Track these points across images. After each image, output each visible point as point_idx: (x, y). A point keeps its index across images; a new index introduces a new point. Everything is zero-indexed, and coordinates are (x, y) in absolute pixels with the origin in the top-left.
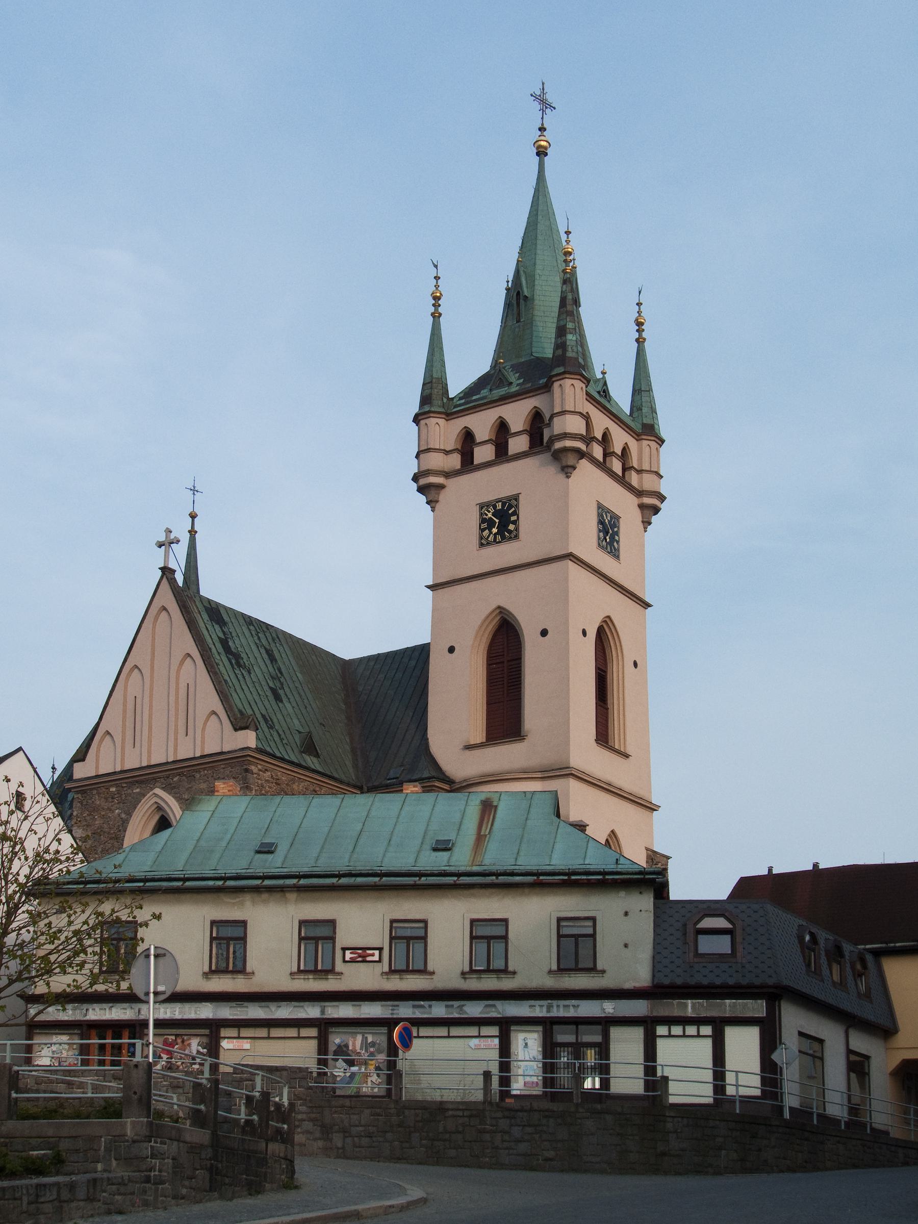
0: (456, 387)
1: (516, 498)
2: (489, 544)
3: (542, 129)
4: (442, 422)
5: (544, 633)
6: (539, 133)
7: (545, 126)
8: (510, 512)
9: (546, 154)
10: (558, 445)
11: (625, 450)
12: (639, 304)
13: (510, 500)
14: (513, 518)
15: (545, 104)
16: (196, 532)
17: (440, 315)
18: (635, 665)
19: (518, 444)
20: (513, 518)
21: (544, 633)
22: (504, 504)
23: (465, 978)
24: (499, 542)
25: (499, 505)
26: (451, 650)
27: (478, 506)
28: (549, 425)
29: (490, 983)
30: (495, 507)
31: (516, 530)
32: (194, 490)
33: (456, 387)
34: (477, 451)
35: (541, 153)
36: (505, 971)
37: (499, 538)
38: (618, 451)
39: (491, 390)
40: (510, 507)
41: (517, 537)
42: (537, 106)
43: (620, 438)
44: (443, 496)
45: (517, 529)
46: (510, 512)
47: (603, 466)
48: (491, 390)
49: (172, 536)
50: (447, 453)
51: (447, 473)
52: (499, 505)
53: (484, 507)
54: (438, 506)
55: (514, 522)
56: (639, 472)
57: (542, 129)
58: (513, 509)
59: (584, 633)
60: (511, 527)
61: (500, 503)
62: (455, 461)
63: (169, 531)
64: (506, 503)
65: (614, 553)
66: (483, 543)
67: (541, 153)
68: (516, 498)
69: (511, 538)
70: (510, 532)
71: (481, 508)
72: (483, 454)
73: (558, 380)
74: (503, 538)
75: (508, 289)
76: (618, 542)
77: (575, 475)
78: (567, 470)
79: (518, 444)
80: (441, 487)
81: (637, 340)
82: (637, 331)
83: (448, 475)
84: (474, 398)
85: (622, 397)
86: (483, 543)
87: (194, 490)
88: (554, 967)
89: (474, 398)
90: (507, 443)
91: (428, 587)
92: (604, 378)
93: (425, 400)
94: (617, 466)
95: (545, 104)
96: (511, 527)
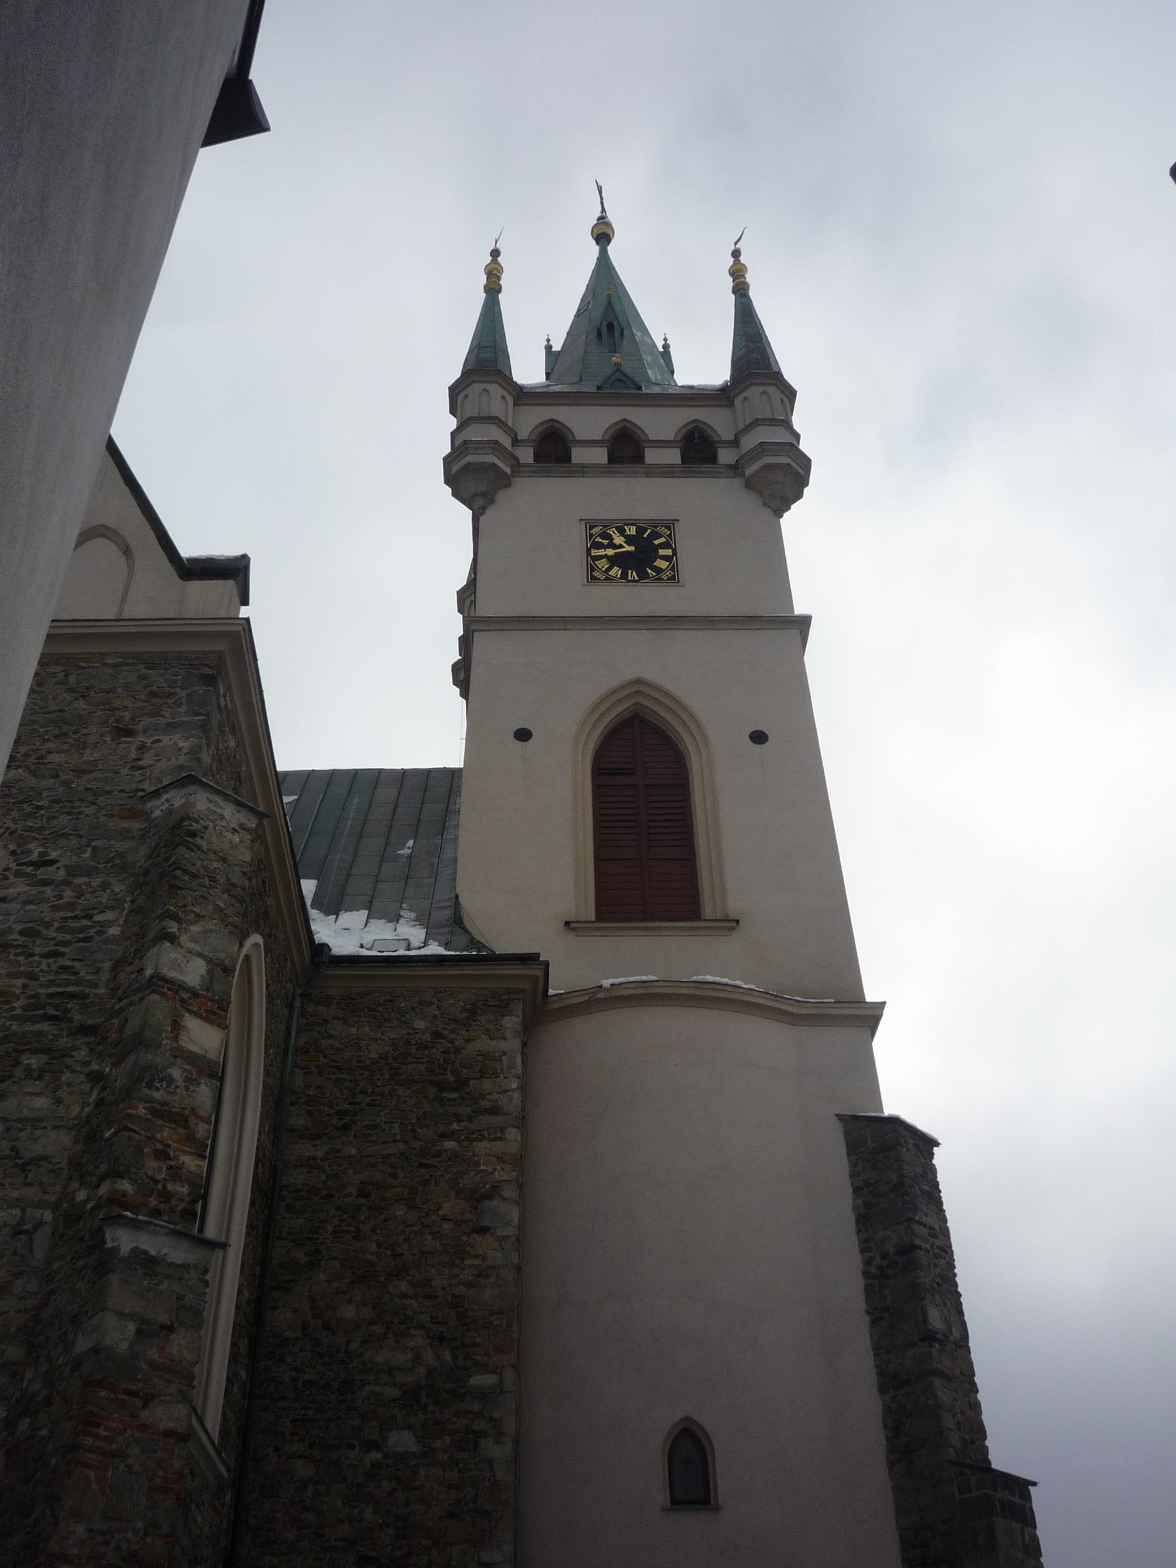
8: (656, 542)
13: (656, 527)
20: (662, 552)
22: (641, 530)
24: (637, 581)
25: (632, 531)
27: (583, 524)
28: (735, 443)
31: (672, 569)
44: (502, 497)
46: (656, 542)
52: (632, 531)
53: (597, 526)
55: (665, 558)
58: (663, 540)
60: (662, 564)
61: (633, 529)
62: (526, 455)
69: (660, 579)
70: (658, 570)
73: (762, 384)
75: (548, 348)
83: (518, 467)
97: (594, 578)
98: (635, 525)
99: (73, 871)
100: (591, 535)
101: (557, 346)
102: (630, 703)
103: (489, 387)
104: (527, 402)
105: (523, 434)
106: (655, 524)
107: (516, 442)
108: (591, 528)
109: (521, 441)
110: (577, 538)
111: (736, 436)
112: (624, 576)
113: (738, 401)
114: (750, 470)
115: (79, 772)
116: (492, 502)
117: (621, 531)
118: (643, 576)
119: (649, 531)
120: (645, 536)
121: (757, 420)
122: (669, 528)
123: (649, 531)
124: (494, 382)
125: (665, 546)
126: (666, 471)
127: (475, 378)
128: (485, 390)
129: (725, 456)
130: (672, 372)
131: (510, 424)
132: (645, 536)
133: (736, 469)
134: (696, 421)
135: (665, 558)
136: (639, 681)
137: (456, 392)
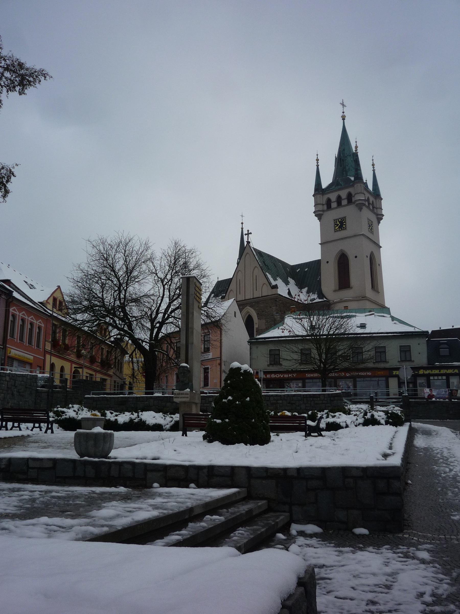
0: (324, 185)
1: (345, 218)
2: (337, 231)
4: (321, 196)
5: (356, 257)
6: (342, 114)
7: (344, 111)
9: (345, 119)
10: (357, 202)
11: (373, 202)
12: (373, 160)
14: (344, 223)
15: (343, 105)
16: (243, 228)
17: (319, 165)
18: (379, 265)
19: (344, 202)
20: (344, 223)
21: (356, 257)
22: (341, 220)
23: (374, 364)
25: (340, 220)
26: (328, 262)
28: (354, 196)
29: (382, 365)
30: (338, 220)
32: (242, 216)
33: (324, 185)
34: (332, 204)
35: (344, 119)
36: (386, 362)
37: (340, 229)
38: (371, 203)
39: (335, 187)
40: (343, 220)
41: (346, 229)
42: (342, 106)
43: (371, 199)
45: (346, 227)
47: (368, 207)
48: (335, 187)
49: (249, 232)
50: (323, 205)
51: (324, 210)
52: (340, 220)
55: (345, 225)
56: (377, 208)
57: (343, 112)
59: (367, 256)
60: (344, 226)
62: (325, 207)
63: (248, 231)
65: (372, 233)
66: (335, 231)
67: (344, 119)
68: (345, 218)
71: (334, 221)
72: (334, 205)
74: (342, 229)
75: (336, 157)
76: (373, 229)
77: (363, 210)
78: (360, 209)
79: (344, 202)
80: (322, 214)
81: (373, 170)
82: (373, 168)
83: (323, 211)
84: (331, 189)
85: (370, 187)
86: (335, 231)
87: (242, 216)
88: (400, 360)
89: (331, 189)
90: (341, 201)
91: (320, 244)
92: (366, 182)
93: (316, 190)
94: (371, 207)
95: (343, 105)
96: (344, 226)
97: (335, 231)
99: (270, 321)
102: (341, 253)
106: (343, 218)
107: (323, 205)
108: (334, 221)
110: (332, 223)
112: (339, 229)
114: (356, 203)
115: (268, 312)
116: (321, 219)
118: (342, 229)
122: (345, 218)
125: (345, 222)
126: (345, 206)
129: (353, 200)
133: (354, 203)
135: (345, 225)
136: (341, 250)
137: (314, 196)
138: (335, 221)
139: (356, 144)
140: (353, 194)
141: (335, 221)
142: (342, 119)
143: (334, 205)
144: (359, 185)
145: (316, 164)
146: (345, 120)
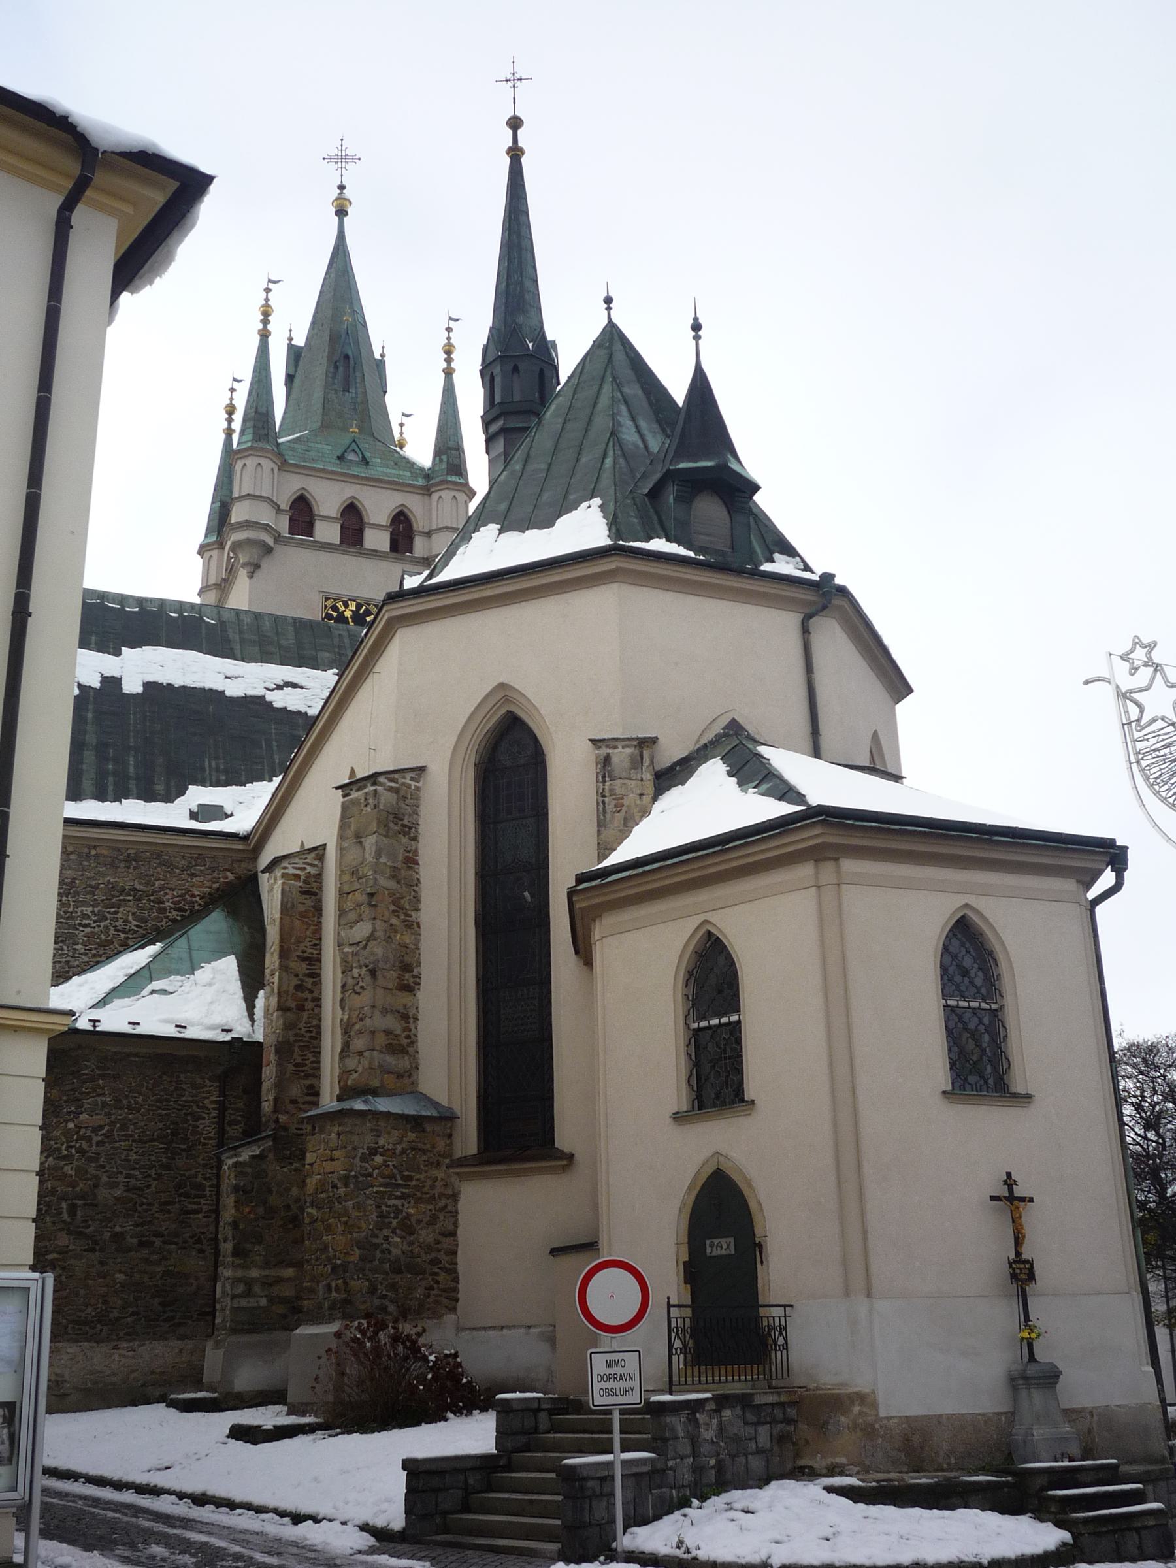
3: (342, 187)
4: (276, 470)
6: (339, 191)
9: (346, 214)
13: (369, 605)
22: (359, 606)
28: (428, 534)
35: (341, 212)
53: (330, 599)
54: (258, 574)
57: (342, 187)
64: (362, 606)
67: (341, 212)
75: (291, 339)
79: (377, 539)
80: (269, 550)
83: (278, 538)
98: (354, 601)
100: (326, 606)
101: (300, 341)
103: (263, 461)
104: (287, 469)
105: (283, 507)
107: (279, 510)
108: (327, 599)
109: (283, 510)
111: (430, 531)
113: (435, 496)
117: (346, 605)
119: (364, 607)
120: (361, 612)
121: (446, 527)
123: (364, 607)
124: (266, 457)
127: (252, 453)
128: (259, 464)
130: (385, 392)
131: (275, 500)
132: (361, 612)
134: (403, 505)
138: (329, 603)
139: (449, 338)
140: (420, 522)
141: (329, 603)
142: (334, 210)
143: (328, 532)
144: (447, 495)
145: (261, 326)
146: (346, 219)
